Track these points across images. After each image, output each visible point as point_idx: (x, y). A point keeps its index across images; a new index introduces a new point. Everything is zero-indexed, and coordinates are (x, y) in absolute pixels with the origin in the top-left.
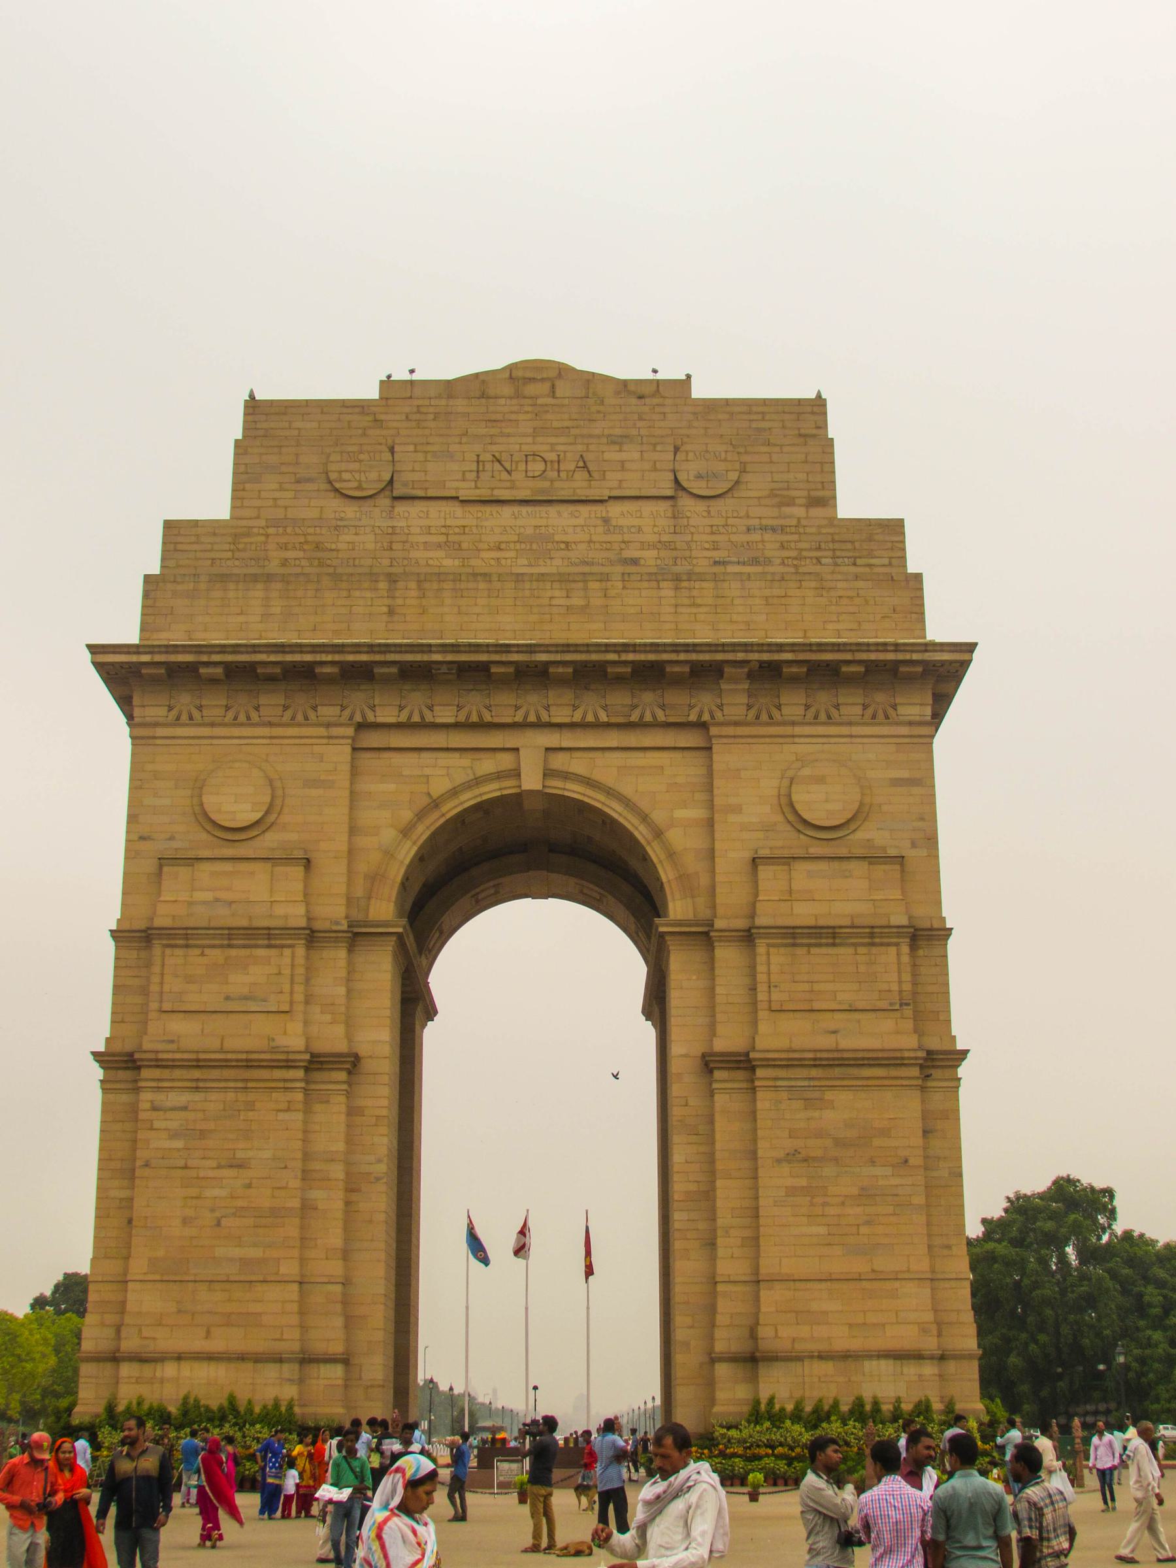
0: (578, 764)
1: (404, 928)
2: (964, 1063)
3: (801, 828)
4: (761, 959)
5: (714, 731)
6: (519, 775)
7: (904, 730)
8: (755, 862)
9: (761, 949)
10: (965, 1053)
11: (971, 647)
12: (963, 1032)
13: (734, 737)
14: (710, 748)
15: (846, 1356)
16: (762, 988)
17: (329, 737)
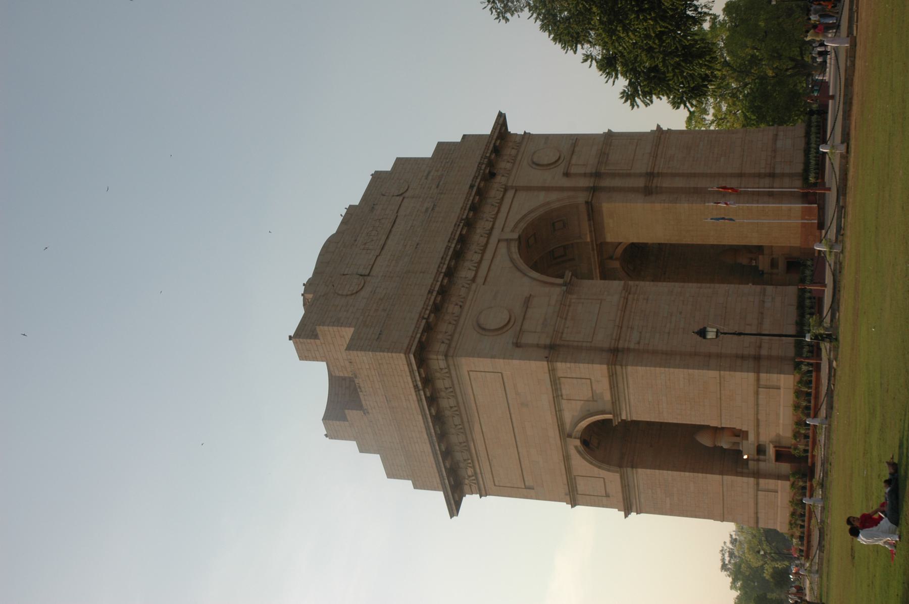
0: (511, 224)
5: (510, 184)
6: (511, 240)
8: (567, 174)
10: (658, 126)
14: (517, 189)
15: (775, 151)
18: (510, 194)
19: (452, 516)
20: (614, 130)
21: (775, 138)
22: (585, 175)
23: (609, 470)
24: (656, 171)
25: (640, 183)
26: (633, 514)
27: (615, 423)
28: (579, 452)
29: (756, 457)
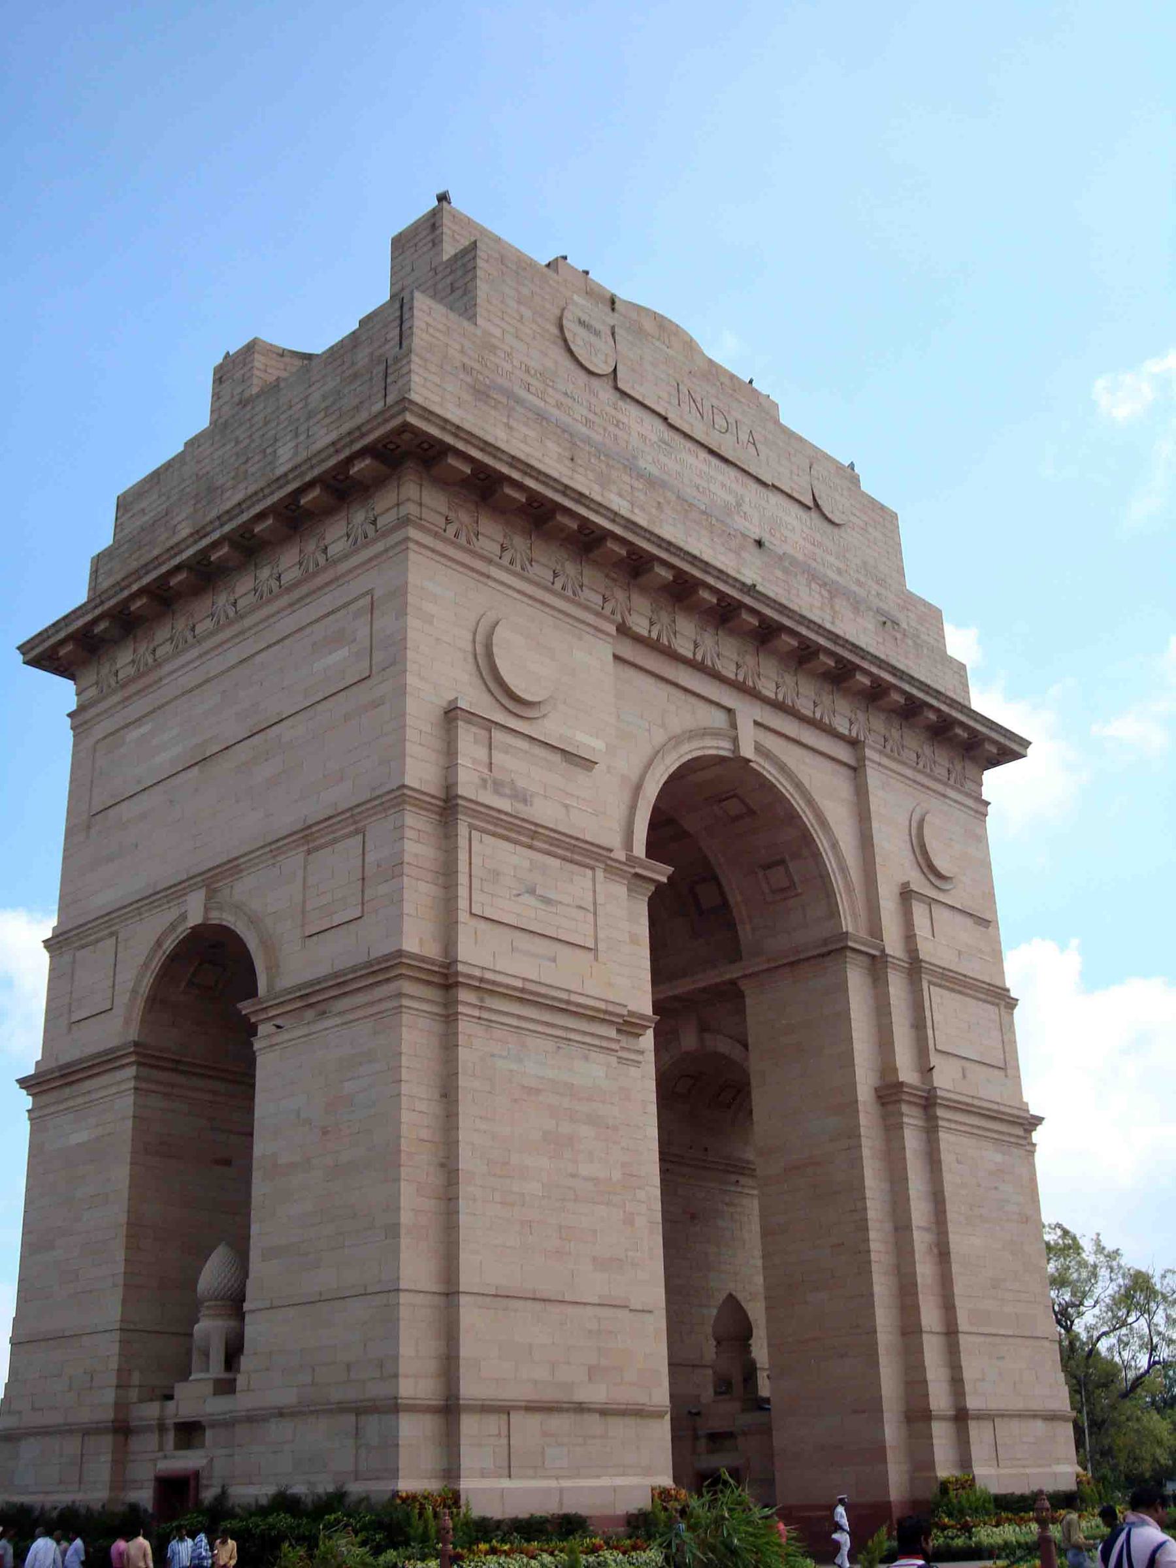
1: (669, 878)
2: (1039, 1128)
3: (925, 870)
4: (926, 993)
5: (868, 753)
6: (735, 740)
7: (970, 802)
8: (906, 895)
9: (925, 985)
10: (1038, 1120)
11: (1026, 744)
12: (1035, 1099)
13: (879, 764)
14: (857, 770)
16: (929, 1024)
17: (596, 628)
18: (843, 753)
19: (23, 649)
20: (1017, 1012)
21: (1052, 1417)
22: (910, 938)
23: (127, 1022)
24: (940, 1112)
25: (907, 1074)
26: (28, 1102)
27: (245, 1007)
28: (173, 927)
29: (170, 1422)
